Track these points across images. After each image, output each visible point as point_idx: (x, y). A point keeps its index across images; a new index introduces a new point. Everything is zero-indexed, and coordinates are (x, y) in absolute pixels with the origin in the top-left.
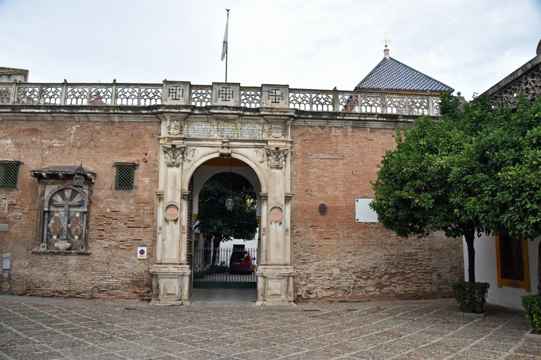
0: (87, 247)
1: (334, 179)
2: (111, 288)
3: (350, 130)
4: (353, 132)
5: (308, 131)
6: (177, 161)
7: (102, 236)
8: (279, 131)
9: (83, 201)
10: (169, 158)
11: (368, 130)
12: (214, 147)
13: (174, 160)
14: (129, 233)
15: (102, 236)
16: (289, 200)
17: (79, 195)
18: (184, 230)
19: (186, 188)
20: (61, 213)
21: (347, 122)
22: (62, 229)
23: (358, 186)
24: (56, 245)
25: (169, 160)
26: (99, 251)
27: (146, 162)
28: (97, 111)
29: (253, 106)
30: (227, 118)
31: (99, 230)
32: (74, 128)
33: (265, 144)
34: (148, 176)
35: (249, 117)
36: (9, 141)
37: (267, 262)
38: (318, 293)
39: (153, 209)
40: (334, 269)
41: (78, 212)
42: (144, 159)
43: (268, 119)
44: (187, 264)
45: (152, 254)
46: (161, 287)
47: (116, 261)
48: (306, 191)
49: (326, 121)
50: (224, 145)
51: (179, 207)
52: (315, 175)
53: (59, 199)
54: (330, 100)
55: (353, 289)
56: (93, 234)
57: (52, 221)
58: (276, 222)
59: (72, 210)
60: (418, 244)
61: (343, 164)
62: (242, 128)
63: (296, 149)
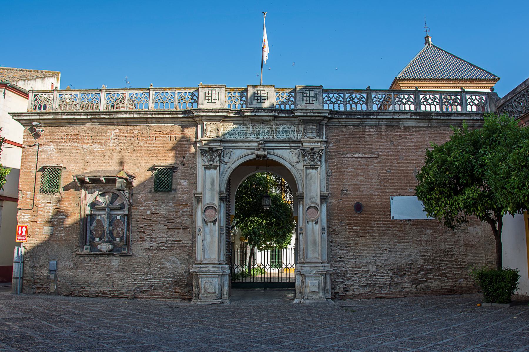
0: (129, 249)
1: (370, 178)
2: (153, 288)
3: (384, 128)
4: (386, 131)
5: (342, 131)
6: (215, 164)
7: (143, 238)
8: (314, 132)
9: (123, 204)
10: (206, 160)
11: (402, 128)
12: (251, 149)
13: (212, 163)
14: (169, 235)
15: (143, 238)
16: (325, 199)
17: (119, 198)
18: (223, 231)
19: (224, 189)
20: (103, 215)
21: (381, 120)
22: (104, 231)
23: (393, 183)
24: (99, 247)
25: (207, 163)
26: (140, 252)
27: (184, 165)
28: (135, 116)
29: (288, 107)
30: (262, 120)
31: (140, 232)
32: (113, 132)
33: (300, 145)
34: (186, 178)
35: (284, 119)
36: (52, 147)
37: (304, 260)
38: (355, 290)
39: (192, 211)
40: (371, 266)
41: (119, 215)
42: (182, 162)
43: (303, 120)
44: (226, 264)
45: (191, 255)
46: (202, 286)
47: (157, 262)
48: (342, 190)
49: (360, 120)
50: (260, 146)
51: (217, 208)
52: (350, 174)
54: (363, 99)
55: (389, 285)
56: (135, 236)
57: (94, 224)
58: (313, 221)
59: (112, 212)
60: (453, 240)
61: (378, 163)
62: (278, 129)
63: (331, 149)
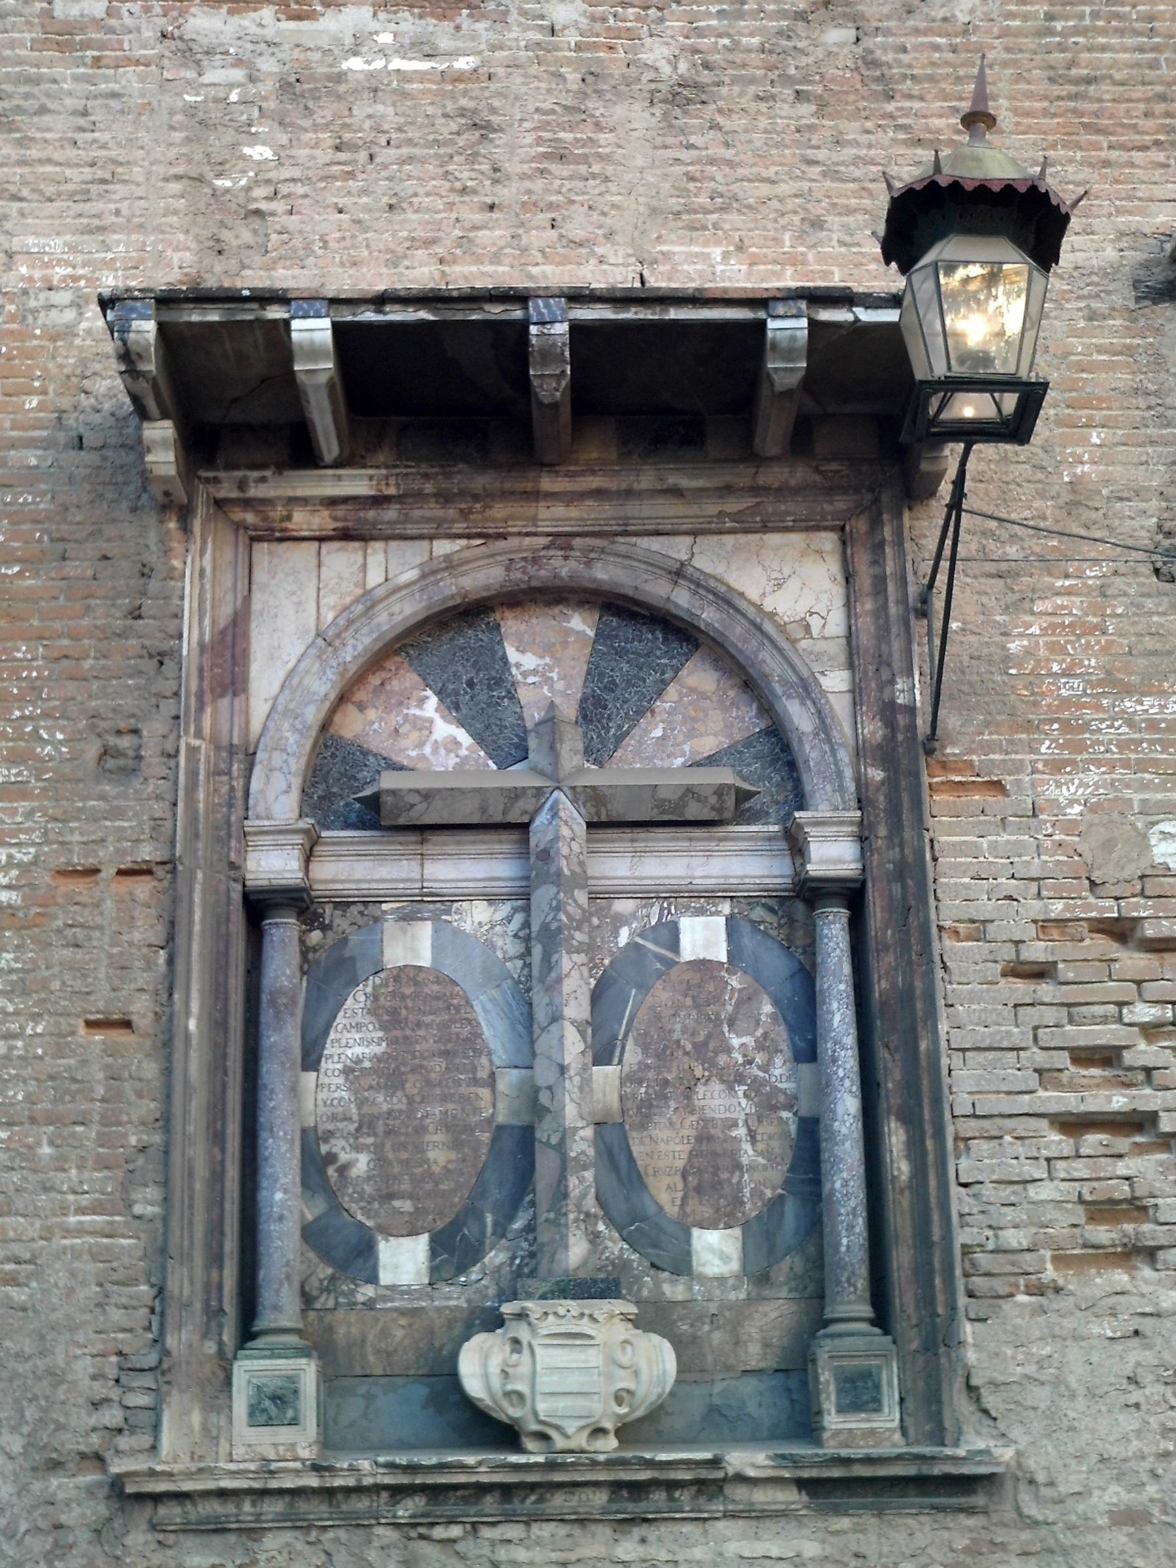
7: (1137, 1208)
15: (1137, 1208)
31: (1074, 1124)
41: (701, 898)
57: (354, 1040)
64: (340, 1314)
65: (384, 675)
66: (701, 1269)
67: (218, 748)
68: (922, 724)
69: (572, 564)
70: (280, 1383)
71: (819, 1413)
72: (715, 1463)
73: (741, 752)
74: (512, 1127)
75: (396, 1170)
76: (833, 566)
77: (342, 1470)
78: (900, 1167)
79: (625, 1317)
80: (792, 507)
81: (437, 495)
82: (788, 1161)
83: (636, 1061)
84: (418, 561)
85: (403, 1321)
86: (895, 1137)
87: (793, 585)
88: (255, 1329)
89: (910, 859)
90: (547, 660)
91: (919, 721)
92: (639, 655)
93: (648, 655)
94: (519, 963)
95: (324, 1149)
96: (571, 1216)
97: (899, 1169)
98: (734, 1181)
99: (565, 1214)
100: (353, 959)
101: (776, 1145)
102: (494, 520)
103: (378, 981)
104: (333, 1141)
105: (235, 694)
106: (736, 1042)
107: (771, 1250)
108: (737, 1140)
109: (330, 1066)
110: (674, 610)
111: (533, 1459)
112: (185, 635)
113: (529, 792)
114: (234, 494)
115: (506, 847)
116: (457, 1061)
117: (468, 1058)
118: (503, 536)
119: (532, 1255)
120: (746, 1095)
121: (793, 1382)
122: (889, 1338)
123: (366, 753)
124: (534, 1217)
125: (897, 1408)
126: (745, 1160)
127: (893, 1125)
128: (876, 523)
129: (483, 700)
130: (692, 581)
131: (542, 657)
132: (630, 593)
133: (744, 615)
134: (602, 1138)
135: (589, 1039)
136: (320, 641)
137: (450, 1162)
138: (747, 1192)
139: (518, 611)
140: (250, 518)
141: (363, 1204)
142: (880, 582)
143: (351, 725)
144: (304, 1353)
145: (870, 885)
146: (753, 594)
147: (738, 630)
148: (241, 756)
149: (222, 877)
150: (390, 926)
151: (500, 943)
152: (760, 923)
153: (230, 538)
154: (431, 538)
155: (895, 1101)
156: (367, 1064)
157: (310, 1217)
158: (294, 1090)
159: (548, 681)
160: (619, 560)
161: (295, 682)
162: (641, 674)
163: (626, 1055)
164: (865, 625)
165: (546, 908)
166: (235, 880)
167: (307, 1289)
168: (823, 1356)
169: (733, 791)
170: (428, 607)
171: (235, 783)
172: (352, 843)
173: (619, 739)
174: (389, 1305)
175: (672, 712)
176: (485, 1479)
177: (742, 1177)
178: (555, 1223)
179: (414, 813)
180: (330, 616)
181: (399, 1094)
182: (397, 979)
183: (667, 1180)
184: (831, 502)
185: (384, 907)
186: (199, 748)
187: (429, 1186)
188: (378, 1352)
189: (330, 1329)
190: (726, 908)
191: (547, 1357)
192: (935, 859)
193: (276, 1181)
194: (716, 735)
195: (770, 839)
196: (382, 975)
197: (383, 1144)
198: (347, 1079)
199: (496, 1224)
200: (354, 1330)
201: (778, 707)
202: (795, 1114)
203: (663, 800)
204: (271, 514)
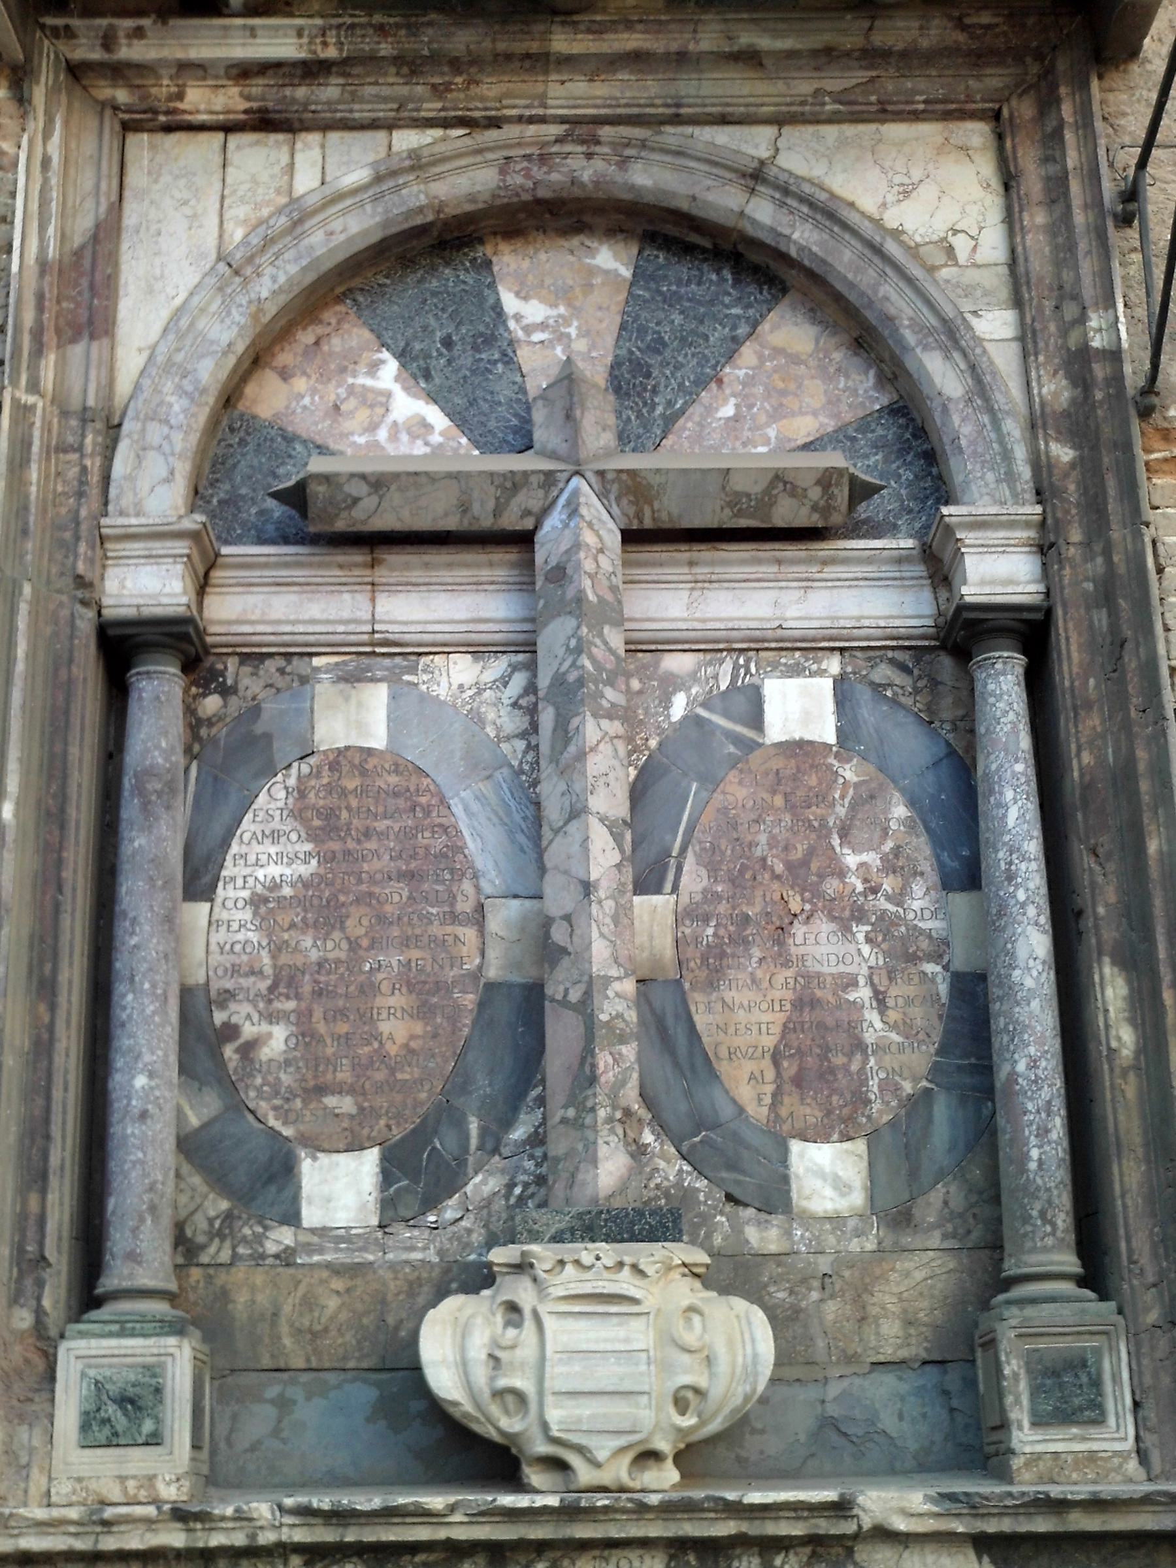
20: (461, 671)
41: (797, 649)
53: (382, 414)
57: (267, 854)
64: (239, 1273)
65: (320, 330)
66: (804, 1203)
67: (65, 414)
68: (1134, 373)
69: (598, 164)
70: (132, 1377)
71: (1003, 1426)
72: (841, 1508)
73: (853, 439)
74: (510, 986)
75: (330, 1051)
76: (986, 167)
77: (223, 1518)
78: (1121, 1036)
79: (690, 1270)
80: (922, 84)
81: (398, 60)
82: (936, 1038)
83: (699, 887)
84: (371, 157)
85: (338, 1284)
86: (1112, 991)
87: (927, 192)
88: (99, 1291)
89: (1122, 569)
90: (562, 310)
91: (1128, 369)
92: (700, 303)
93: (712, 302)
94: (521, 745)
95: (219, 1017)
96: (602, 1113)
97: (1119, 1039)
98: (854, 1067)
99: (593, 1110)
100: (268, 737)
101: (918, 1014)
102: (483, 99)
103: (305, 769)
104: (233, 1006)
105: (92, 337)
106: (851, 860)
107: (914, 1174)
108: (856, 1006)
109: (231, 893)
110: (750, 230)
111: (540, 1501)
112: (16, 244)
113: (534, 479)
114: (97, 55)
115: (501, 574)
116: (426, 886)
117: (443, 882)
118: (495, 123)
119: (541, 1180)
120: (868, 940)
121: (953, 1378)
122: (1112, 1305)
123: (290, 439)
124: (544, 1122)
125: (1130, 1419)
126: (869, 1037)
127: (1107, 970)
128: (1048, 103)
129: (466, 365)
130: (777, 187)
131: (554, 305)
132: (685, 206)
133: (855, 233)
134: (650, 1004)
135: (628, 847)
136: (222, 267)
137: (413, 1037)
138: (874, 1084)
139: (519, 243)
140: (122, 96)
141: (277, 1102)
142: (1057, 191)
143: (269, 398)
144: (177, 1329)
145: (1059, 612)
146: (868, 204)
147: (847, 255)
148: (99, 425)
149: (64, 598)
150: (324, 690)
151: (491, 715)
152: (885, 686)
153: (92, 123)
154: (390, 126)
155: (1109, 934)
156: (287, 891)
157: (194, 1121)
158: (170, 921)
159: (563, 338)
160: (668, 158)
161: (184, 323)
162: (701, 329)
163: (684, 879)
164: (1037, 244)
165: (561, 652)
166: (84, 603)
167: (189, 1232)
168: (1007, 1337)
169: (845, 480)
170: (385, 224)
171: (88, 462)
172: (266, 566)
173: (670, 421)
174: (316, 1258)
175: (748, 382)
176: (461, 1534)
177: (865, 1061)
178: (577, 1124)
179: (358, 513)
180: (239, 234)
181: (337, 935)
182: (334, 766)
183: (749, 1067)
184: (978, 77)
185: (317, 661)
186: (34, 406)
187: (380, 1075)
188: (298, 1332)
189: (224, 1295)
190: (834, 665)
191: (562, 1332)
192: (1160, 570)
193: (138, 1057)
194: (815, 414)
195: (899, 561)
196: (312, 760)
197: (310, 1013)
198: (255, 914)
199: (484, 1132)
200: (260, 1298)
201: (910, 365)
202: (946, 968)
203: (736, 493)
204: (154, 91)
